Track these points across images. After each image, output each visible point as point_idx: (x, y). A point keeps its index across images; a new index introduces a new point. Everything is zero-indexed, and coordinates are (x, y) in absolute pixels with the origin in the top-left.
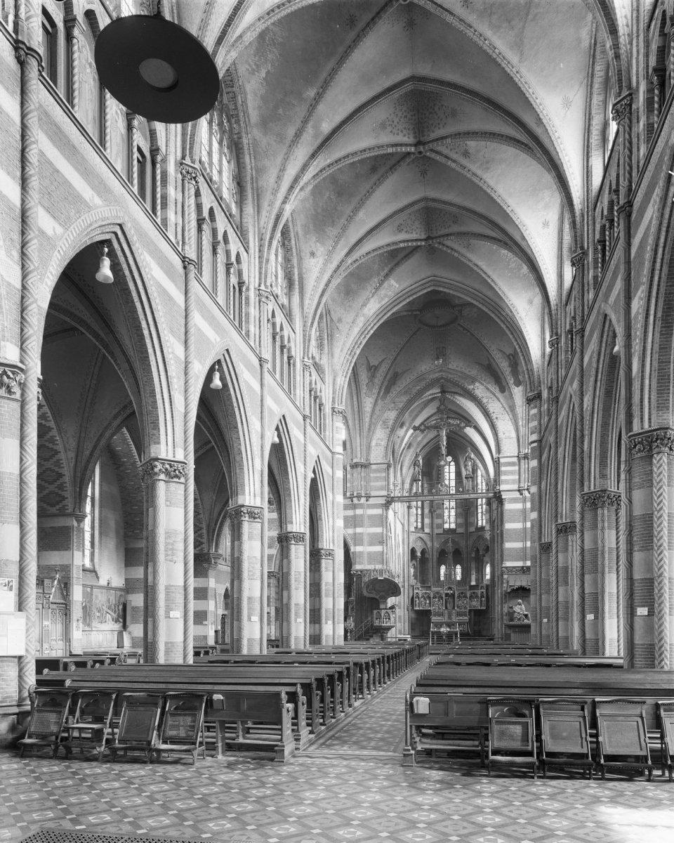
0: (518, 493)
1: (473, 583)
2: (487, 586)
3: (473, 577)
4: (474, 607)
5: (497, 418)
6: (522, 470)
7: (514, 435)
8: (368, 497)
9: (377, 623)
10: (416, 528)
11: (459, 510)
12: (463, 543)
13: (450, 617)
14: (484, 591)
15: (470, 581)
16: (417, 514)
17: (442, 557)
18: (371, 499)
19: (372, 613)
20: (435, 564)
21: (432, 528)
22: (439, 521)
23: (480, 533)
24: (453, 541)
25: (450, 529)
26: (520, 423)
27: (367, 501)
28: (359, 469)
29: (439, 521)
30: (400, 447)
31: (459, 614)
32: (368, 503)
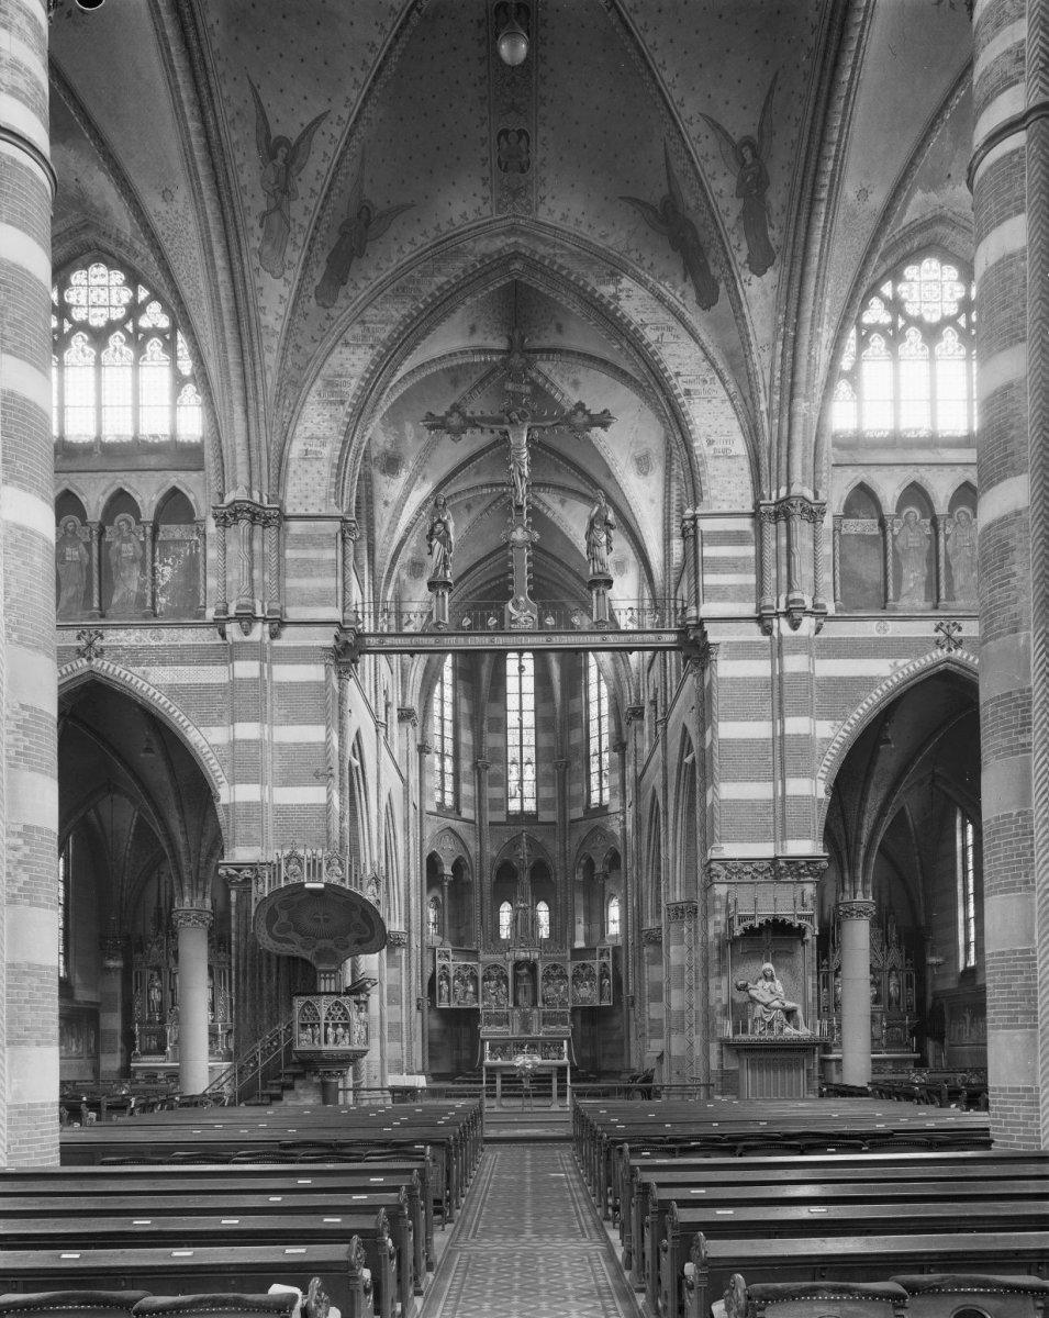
0: (755, 627)
1: (580, 944)
2: (616, 949)
3: (580, 929)
4: (584, 1000)
5: (688, 392)
6: (769, 555)
7: (739, 447)
9: (304, 1042)
10: (441, 805)
11: (546, 767)
12: (554, 848)
13: (526, 1027)
14: (609, 960)
15: (573, 939)
16: (442, 772)
17: (506, 880)
18: (287, 632)
19: (290, 1007)
20: (488, 898)
21: (480, 808)
22: (496, 792)
23: (597, 821)
24: (532, 842)
26: (763, 407)
27: (274, 635)
28: (244, 524)
29: (496, 792)
30: (391, 531)
31: (547, 1020)
32: (276, 643)
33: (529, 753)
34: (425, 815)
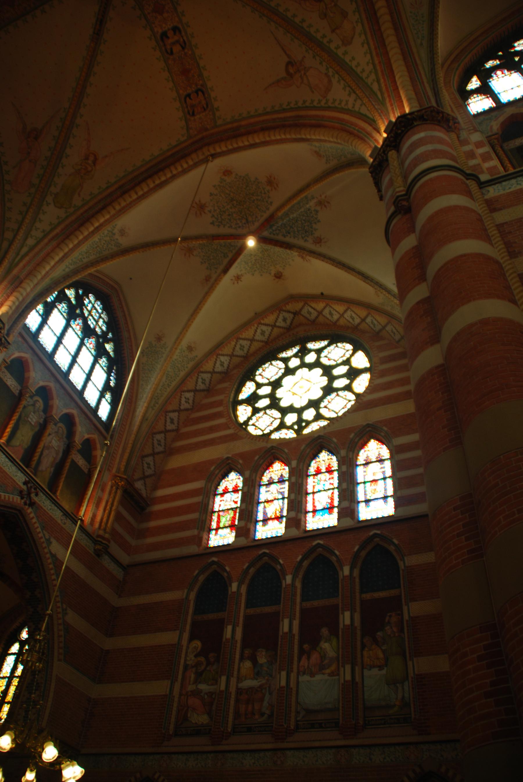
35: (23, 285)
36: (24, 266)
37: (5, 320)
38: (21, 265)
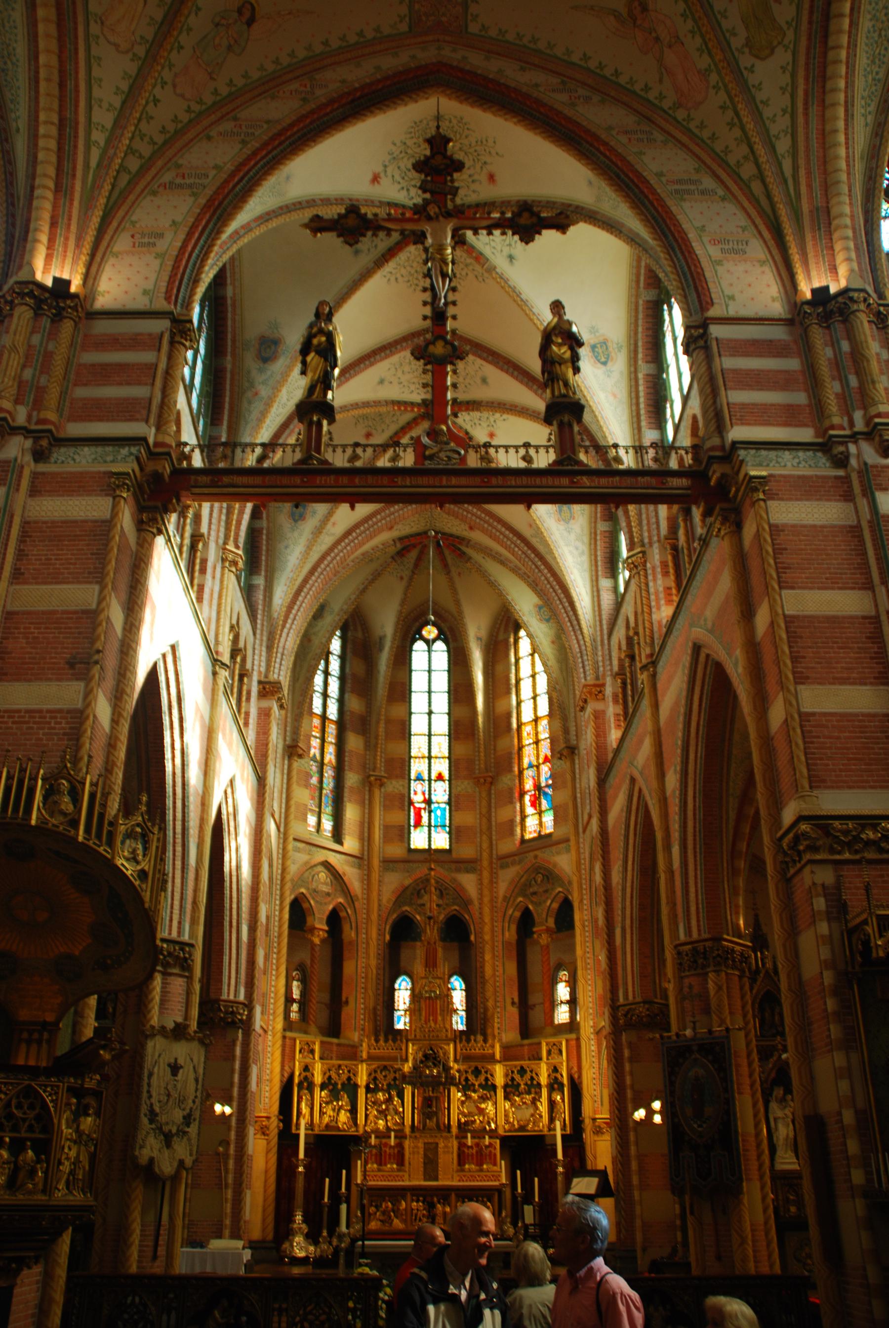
8: (46, 443)
13: (431, 1167)
18: (60, 453)
22: (396, 817)
25: (429, 851)
29: (396, 817)
33: (442, 767)
34: (291, 845)
35: (834, 211)
36: (809, 186)
37: (858, 284)
38: (803, 189)
